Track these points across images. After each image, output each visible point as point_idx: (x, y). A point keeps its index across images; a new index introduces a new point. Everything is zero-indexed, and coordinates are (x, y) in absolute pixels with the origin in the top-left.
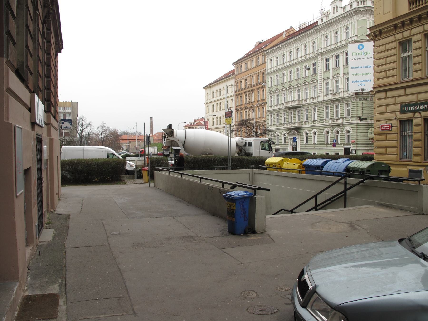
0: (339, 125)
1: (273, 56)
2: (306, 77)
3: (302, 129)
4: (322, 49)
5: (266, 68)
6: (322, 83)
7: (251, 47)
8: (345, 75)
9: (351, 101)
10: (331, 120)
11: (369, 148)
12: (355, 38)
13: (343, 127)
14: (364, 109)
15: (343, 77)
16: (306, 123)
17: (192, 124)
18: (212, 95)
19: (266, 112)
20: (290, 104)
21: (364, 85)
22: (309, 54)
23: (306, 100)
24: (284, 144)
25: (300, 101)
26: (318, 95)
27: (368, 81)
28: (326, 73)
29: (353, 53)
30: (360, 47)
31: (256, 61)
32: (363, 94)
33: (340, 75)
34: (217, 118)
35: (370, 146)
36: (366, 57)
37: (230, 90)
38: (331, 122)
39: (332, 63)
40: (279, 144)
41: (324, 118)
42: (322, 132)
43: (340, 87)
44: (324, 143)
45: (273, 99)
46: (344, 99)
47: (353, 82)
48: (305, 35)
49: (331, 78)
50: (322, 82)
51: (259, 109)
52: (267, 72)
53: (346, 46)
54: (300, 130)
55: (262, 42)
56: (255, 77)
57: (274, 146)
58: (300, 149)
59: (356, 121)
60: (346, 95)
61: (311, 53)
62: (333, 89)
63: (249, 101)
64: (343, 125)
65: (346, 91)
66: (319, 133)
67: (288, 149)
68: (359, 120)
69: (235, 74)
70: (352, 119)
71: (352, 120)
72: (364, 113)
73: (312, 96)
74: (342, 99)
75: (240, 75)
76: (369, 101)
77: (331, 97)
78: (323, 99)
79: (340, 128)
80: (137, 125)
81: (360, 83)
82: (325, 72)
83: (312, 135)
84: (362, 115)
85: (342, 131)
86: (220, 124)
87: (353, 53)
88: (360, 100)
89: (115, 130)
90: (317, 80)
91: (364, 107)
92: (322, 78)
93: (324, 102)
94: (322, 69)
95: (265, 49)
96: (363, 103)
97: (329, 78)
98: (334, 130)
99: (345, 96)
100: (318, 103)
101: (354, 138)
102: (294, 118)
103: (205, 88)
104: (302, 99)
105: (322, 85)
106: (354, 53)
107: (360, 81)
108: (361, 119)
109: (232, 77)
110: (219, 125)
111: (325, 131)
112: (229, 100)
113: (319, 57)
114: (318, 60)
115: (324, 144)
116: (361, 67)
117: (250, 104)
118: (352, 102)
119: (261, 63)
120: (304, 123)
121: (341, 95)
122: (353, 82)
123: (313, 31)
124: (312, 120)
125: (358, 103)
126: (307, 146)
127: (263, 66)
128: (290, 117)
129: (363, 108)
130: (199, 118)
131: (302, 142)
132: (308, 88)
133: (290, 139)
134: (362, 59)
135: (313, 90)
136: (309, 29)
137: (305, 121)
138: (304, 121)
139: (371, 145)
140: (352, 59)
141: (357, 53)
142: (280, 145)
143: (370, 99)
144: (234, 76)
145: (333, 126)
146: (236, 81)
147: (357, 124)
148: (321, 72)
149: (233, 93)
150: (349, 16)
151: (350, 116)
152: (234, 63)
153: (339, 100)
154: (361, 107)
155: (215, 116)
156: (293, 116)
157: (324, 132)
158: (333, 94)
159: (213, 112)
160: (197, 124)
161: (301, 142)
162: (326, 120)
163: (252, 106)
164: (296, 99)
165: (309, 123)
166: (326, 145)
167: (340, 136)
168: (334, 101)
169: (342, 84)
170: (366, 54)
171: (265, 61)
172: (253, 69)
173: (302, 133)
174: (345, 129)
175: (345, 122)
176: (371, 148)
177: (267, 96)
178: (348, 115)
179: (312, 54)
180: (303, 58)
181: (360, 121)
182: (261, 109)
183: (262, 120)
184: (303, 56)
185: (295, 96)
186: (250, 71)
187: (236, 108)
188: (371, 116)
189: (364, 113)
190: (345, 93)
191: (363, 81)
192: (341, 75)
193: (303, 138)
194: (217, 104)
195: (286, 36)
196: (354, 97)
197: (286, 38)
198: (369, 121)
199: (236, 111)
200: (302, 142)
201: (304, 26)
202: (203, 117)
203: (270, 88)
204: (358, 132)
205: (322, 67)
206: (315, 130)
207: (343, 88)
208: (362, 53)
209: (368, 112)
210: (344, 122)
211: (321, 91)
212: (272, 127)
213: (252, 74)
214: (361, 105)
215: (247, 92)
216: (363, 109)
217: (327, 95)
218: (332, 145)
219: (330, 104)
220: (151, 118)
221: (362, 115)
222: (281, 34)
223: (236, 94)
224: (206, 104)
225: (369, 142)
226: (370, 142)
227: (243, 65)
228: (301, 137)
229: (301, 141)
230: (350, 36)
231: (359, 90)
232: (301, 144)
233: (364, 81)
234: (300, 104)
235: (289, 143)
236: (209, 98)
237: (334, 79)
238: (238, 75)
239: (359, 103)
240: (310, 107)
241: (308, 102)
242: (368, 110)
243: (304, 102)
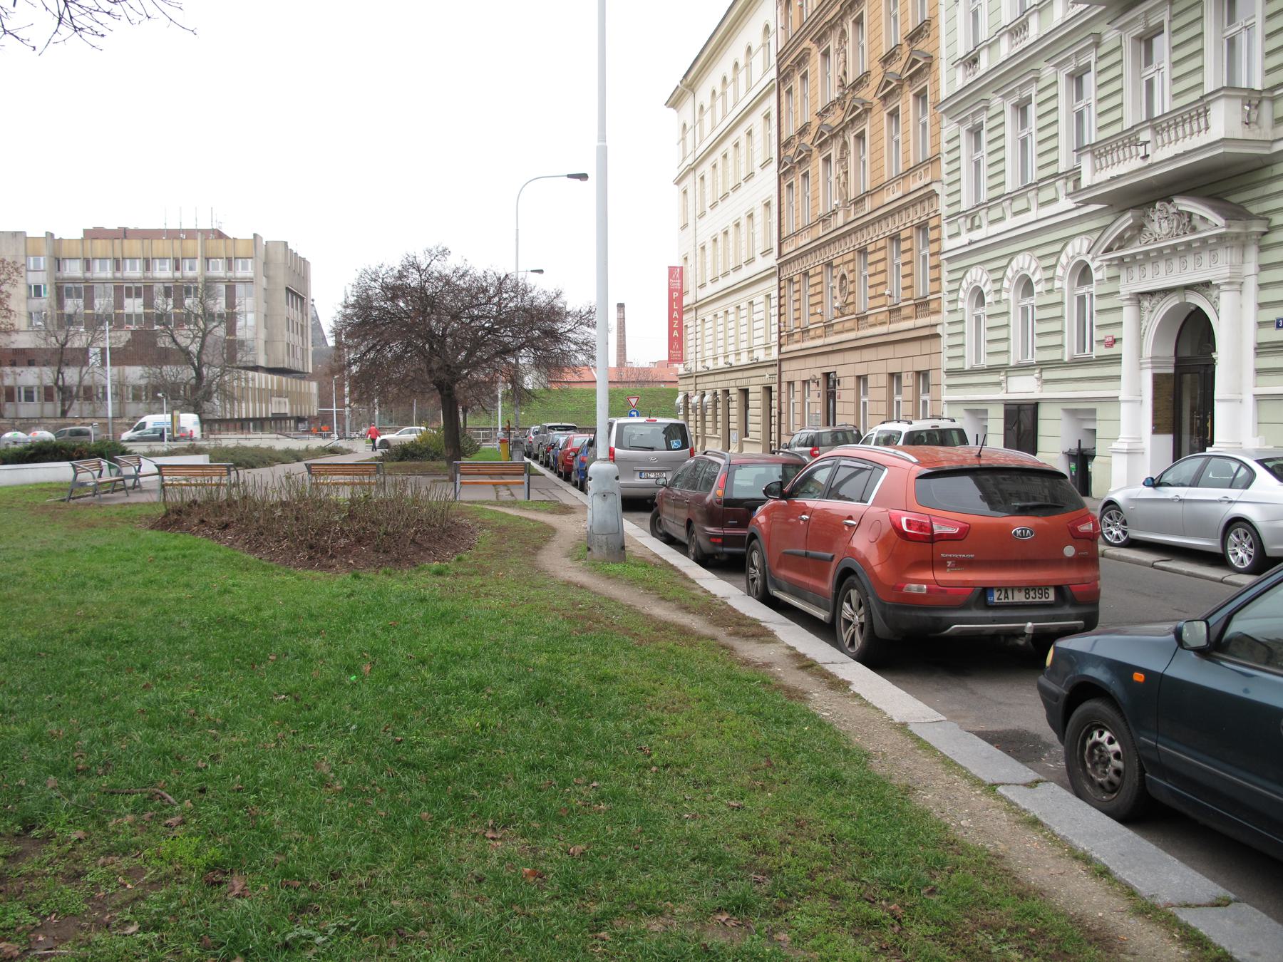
3: (1267, 173)
24: (1076, 363)
40: (1039, 364)
57: (999, 384)
58: (1259, 398)
67: (1115, 400)
128: (1135, 85)
133: (1140, 297)
142: (1043, 365)
161: (1261, 324)
183: (913, 187)
212: (979, 227)
228: (1263, 267)
229: (1262, 306)
235: (1126, 349)
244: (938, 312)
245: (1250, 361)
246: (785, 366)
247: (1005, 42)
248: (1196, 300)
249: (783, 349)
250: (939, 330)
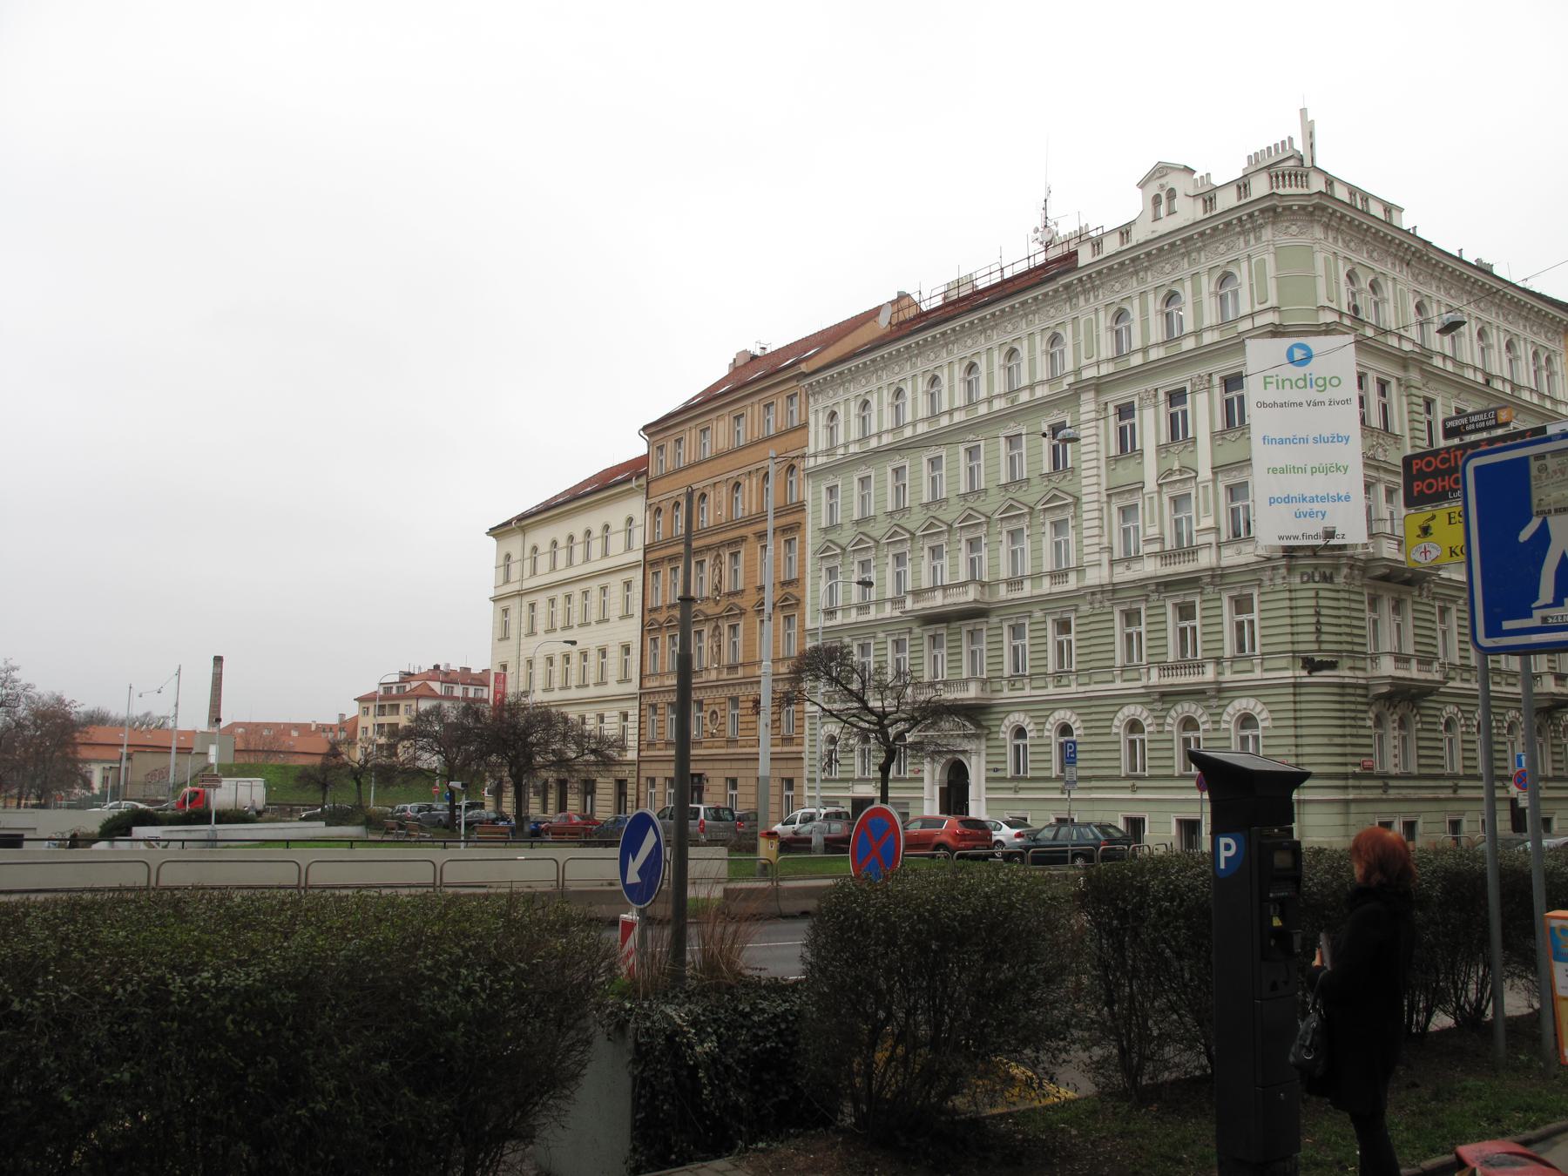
0: (1203, 692)
1: (845, 402)
2: (1014, 482)
4: (1098, 364)
5: (806, 449)
6: (1101, 510)
7: (713, 370)
8: (1115, 494)
9: (1260, 586)
10: (1154, 672)
11: (1351, 797)
12: (1271, 318)
13: (1221, 699)
14: (1323, 620)
15: (1214, 481)
16: (1018, 685)
17: (394, 691)
18: (528, 563)
19: (805, 637)
20: (938, 601)
21: (1324, 516)
22: (951, 412)
23: (1015, 582)
25: (987, 588)
26: (1086, 559)
27: (1339, 499)
28: (1120, 464)
29: (1268, 380)
30: (1298, 355)
31: (756, 420)
32: (1315, 555)
33: (1197, 473)
34: (584, 655)
35: (1354, 787)
36: (1320, 397)
37: (617, 542)
38: (1155, 678)
39: (1151, 426)
41: (1118, 662)
42: (1108, 723)
43: (1198, 524)
44: (1116, 772)
45: (840, 578)
46: (1222, 576)
47: (1272, 501)
48: (865, 363)
49: (1151, 485)
50: (1105, 505)
51: (654, 640)
52: (811, 462)
53: (1236, 346)
54: (987, 717)
55: (758, 352)
56: (750, 486)
59: (1289, 673)
60: (1230, 557)
61: (1042, 383)
62: (1162, 533)
63: (717, 589)
64: (1220, 690)
65: (1228, 543)
66: (1085, 728)
67: (922, 798)
68: (1304, 668)
69: (646, 472)
70: (1267, 665)
71: (1265, 667)
72: (1324, 637)
73: (1048, 566)
74: (1213, 576)
75: (672, 478)
76: (1342, 587)
77: (1150, 568)
78: (1111, 575)
79: (1206, 704)
80: (178, 673)
81: (1306, 507)
82: (1116, 459)
83: (1049, 737)
84: (1315, 647)
85: (1041, 727)
86: (566, 687)
87: (1268, 380)
88: (1303, 582)
89: (60, 701)
90: (1077, 500)
91: (1324, 611)
92: (1104, 486)
93: (1114, 591)
94: (1102, 447)
95: (804, 367)
96: (1317, 594)
97: (1140, 485)
98: (1173, 713)
99: (1224, 563)
100: (1084, 596)
101: (1284, 751)
102: (949, 661)
103: (499, 532)
104: (993, 577)
105: (1101, 519)
106: (1274, 380)
107: (1304, 499)
108: (1311, 665)
109: (634, 484)
110: (573, 688)
111: (1127, 714)
112: (615, 583)
113: (1088, 396)
114: (1082, 409)
115: (1119, 776)
116: (1305, 440)
117: (724, 604)
118: (1263, 590)
119: (784, 429)
120: (1005, 682)
121: (1206, 559)
122: (1272, 501)
123: (1056, 291)
124: (1050, 670)
125: (1294, 595)
127: (794, 438)
129: (1318, 614)
130: (420, 668)
131: (996, 770)
132: (984, 541)
134: (1305, 404)
135: (1051, 539)
136: (1032, 282)
137: (1012, 676)
138: (1006, 673)
139: (1356, 783)
140: (1263, 405)
141: (1283, 381)
143: (1345, 577)
144: (643, 481)
145: (1168, 696)
146: (649, 502)
147: (1295, 685)
148: (1098, 459)
149: (638, 556)
150: (1238, 229)
151: (1144, 662)
152: (645, 428)
153: (1198, 579)
154: (1312, 611)
155: (574, 643)
156: (949, 654)
157: (1116, 722)
158: (1164, 556)
159: (532, 633)
160: (416, 693)
161: (987, 770)
162: (1124, 669)
163: (731, 609)
164: (963, 576)
165: (1035, 684)
166: (1128, 783)
167: (1204, 739)
168: (1167, 585)
169: (1206, 510)
170: (1325, 384)
171: (803, 418)
172: (739, 454)
173: (994, 729)
174: (1230, 709)
175: (1228, 676)
176: (1358, 797)
177: (809, 568)
178: (1130, 659)
179: (963, 412)
180: (998, 405)
181: (1309, 672)
182: (664, 642)
184: (999, 396)
185: (956, 566)
186: (723, 459)
187: (647, 618)
188: (1352, 652)
189: (1324, 637)
190: (1226, 552)
191: (1317, 497)
192: (1205, 473)
193: (1002, 751)
194: (552, 601)
195: (894, 322)
196: (1274, 568)
197: (891, 331)
198: (1348, 673)
199: (645, 633)
200: (996, 770)
201: (961, 289)
202: (437, 667)
203: (826, 530)
204: (1299, 723)
205: (1102, 439)
206: (1062, 715)
207: (1217, 530)
208: (1305, 380)
209: (1340, 634)
210: (1221, 678)
211: (1099, 544)
213: (734, 474)
214: (1313, 603)
215: (708, 548)
216: (1318, 622)
217: (1128, 559)
218: (1193, 783)
219: (1147, 598)
220: (218, 660)
221: (1315, 647)
222: (874, 314)
223: (650, 557)
224: (495, 600)
225: (1350, 769)
226: (1357, 770)
227: (690, 435)
229: (987, 762)
230: (1245, 309)
231: (1301, 537)
232: (988, 780)
233: (1323, 499)
234: (987, 598)
236: (515, 575)
237: (1165, 489)
238: (662, 477)
239: (1299, 594)
240: (881, 635)
241: (1027, 590)
242: (1340, 626)
243: (1003, 593)
244: (802, 745)
246: (643, 766)
247: (854, 612)
248: (961, 757)
249: (642, 754)
250: (803, 755)
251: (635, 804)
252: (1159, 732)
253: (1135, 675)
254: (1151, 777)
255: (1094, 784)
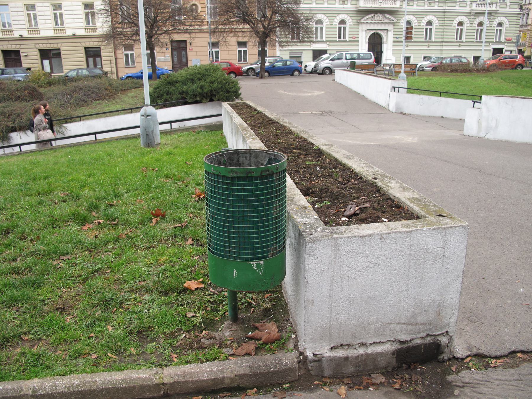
3: (396, 13)
38: (474, 7)
40: (326, 41)
126: (410, 45)
166: (458, 44)
200: (397, 38)
229: (394, 35)
232: (394, 42)
245: (392, 44)
251: (114, 62)
252: (470, 26)
253: (465, 5)
254: (466, 42)
255: (444, 44)
